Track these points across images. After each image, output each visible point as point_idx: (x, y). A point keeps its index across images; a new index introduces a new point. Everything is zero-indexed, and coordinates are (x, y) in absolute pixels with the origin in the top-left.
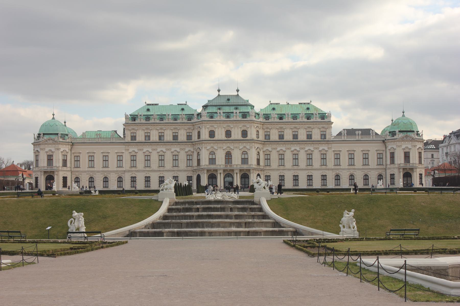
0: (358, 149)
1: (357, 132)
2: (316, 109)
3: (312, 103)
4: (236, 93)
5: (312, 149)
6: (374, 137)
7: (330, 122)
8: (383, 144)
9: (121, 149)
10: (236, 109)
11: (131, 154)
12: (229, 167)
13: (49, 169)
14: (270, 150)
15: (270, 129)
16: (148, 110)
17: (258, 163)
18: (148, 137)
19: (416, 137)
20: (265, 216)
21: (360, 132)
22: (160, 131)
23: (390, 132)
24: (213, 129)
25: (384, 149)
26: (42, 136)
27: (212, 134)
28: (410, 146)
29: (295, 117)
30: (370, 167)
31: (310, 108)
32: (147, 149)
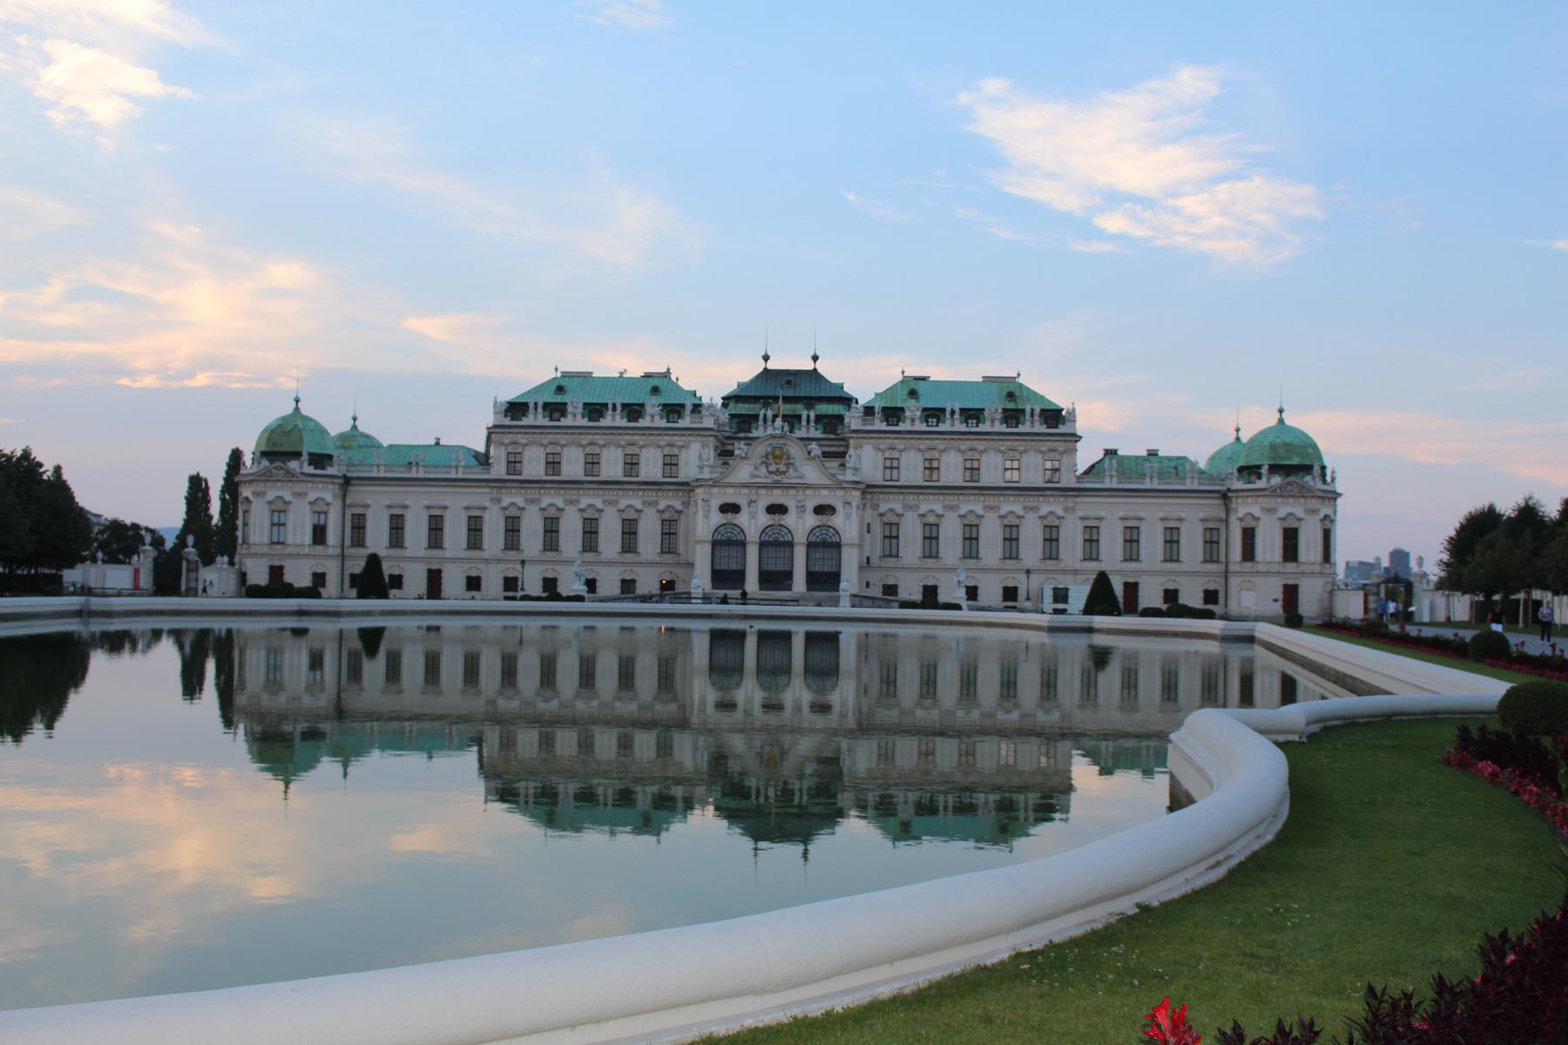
0: (1152, 517)
3: (1020, 380)
5: (1020, 512)
7: (1074, 435)
8: (1220, 502)
9: (480, 497)
11: (508, 513)
14: (899, 509)
15: (901, 451)
16: (560, 390)
18: (553, 464)
19: (1319, 485)
22: (588, 450)
23: (1241, 470)
25: (1223, 515)
28: (1299, 512)
29: (972, 415)
30: (1183, 567)
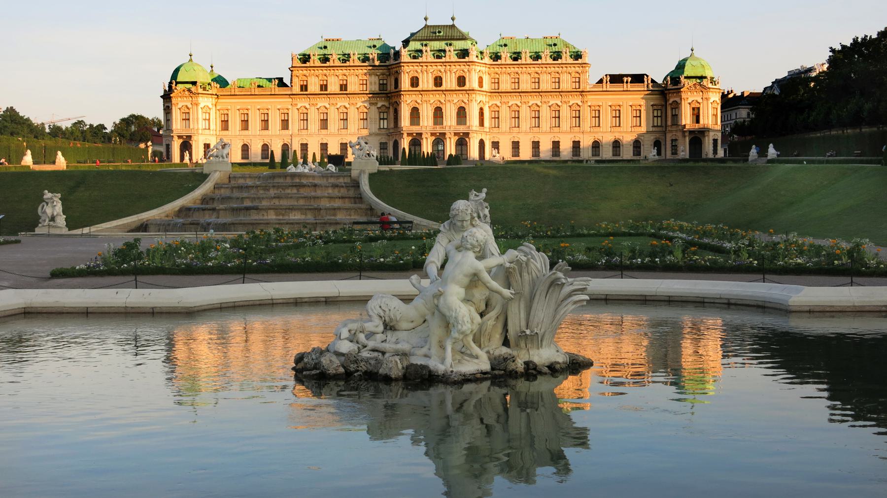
1: (625, 79)
2: (567, 46)
4: (450, 23)
6: (651, 85)
10: (450, 45)
12: (438, 129)
13: (185, 133)
17: (482, 123)
20: (359, 198)
21: (630, 79)
24: (416, 75)
25: (663, 103)
26: (174, 85)
27: (415, 82)
29: (537, 57)
31: (558, 44)
32: (322, 102)
